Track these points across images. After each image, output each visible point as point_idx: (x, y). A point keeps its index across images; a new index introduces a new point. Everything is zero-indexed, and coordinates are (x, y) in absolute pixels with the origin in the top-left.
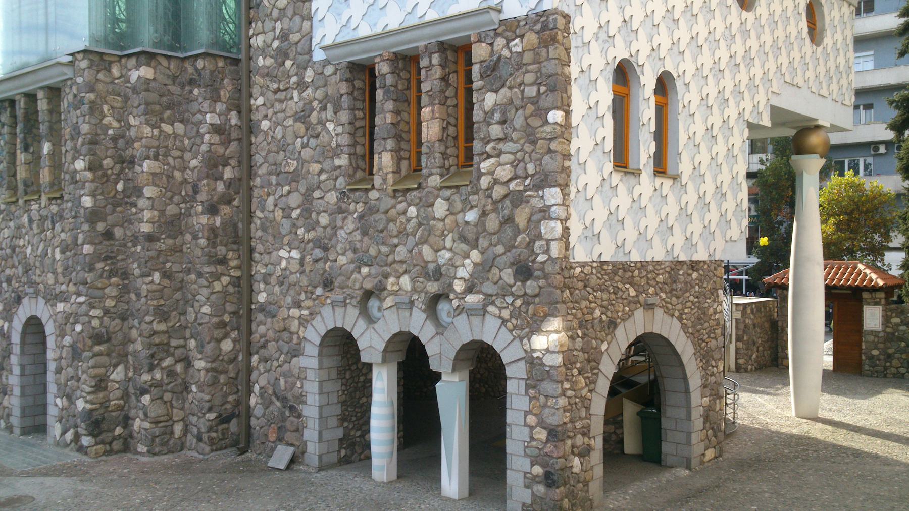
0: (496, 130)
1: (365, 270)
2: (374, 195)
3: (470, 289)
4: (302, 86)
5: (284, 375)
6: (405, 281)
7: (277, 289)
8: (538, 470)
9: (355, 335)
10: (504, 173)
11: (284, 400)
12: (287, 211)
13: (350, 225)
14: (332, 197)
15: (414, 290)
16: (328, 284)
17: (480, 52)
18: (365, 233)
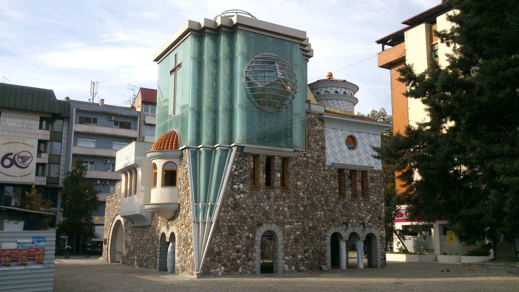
0: (373, 190)
1: (344, 218)
2: (346, 200)
3: (369, 222)
4: (324, 170)
5: (320, 246)
6: (354, 220)
7: (316, 222)
8: (383, 257)
9: (341, 233)
10: (375, 199)
11: (320, 253)
12: (320, 202)
13: (340, 207)
14: (334, 199)
15: (357, 222)
16: (333, 221)
17: (369, 174)
18: (343, 208)
